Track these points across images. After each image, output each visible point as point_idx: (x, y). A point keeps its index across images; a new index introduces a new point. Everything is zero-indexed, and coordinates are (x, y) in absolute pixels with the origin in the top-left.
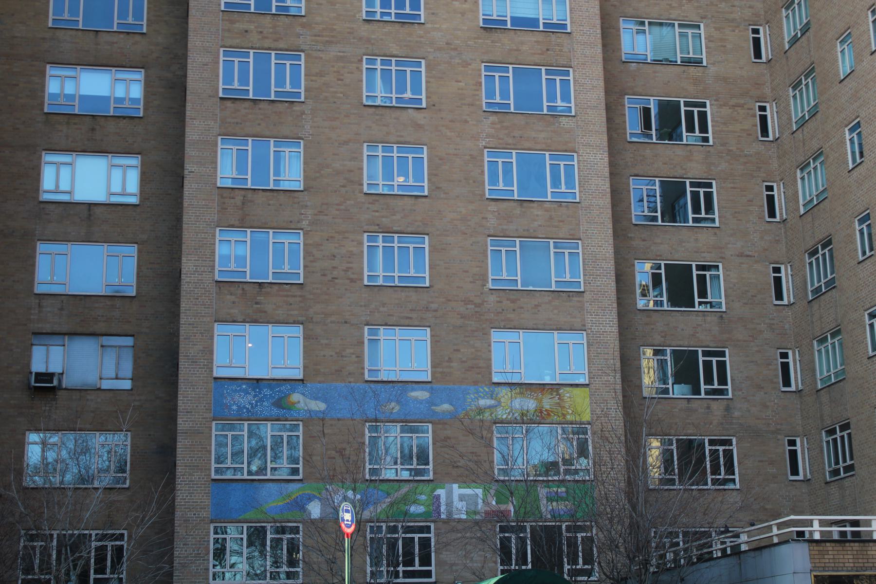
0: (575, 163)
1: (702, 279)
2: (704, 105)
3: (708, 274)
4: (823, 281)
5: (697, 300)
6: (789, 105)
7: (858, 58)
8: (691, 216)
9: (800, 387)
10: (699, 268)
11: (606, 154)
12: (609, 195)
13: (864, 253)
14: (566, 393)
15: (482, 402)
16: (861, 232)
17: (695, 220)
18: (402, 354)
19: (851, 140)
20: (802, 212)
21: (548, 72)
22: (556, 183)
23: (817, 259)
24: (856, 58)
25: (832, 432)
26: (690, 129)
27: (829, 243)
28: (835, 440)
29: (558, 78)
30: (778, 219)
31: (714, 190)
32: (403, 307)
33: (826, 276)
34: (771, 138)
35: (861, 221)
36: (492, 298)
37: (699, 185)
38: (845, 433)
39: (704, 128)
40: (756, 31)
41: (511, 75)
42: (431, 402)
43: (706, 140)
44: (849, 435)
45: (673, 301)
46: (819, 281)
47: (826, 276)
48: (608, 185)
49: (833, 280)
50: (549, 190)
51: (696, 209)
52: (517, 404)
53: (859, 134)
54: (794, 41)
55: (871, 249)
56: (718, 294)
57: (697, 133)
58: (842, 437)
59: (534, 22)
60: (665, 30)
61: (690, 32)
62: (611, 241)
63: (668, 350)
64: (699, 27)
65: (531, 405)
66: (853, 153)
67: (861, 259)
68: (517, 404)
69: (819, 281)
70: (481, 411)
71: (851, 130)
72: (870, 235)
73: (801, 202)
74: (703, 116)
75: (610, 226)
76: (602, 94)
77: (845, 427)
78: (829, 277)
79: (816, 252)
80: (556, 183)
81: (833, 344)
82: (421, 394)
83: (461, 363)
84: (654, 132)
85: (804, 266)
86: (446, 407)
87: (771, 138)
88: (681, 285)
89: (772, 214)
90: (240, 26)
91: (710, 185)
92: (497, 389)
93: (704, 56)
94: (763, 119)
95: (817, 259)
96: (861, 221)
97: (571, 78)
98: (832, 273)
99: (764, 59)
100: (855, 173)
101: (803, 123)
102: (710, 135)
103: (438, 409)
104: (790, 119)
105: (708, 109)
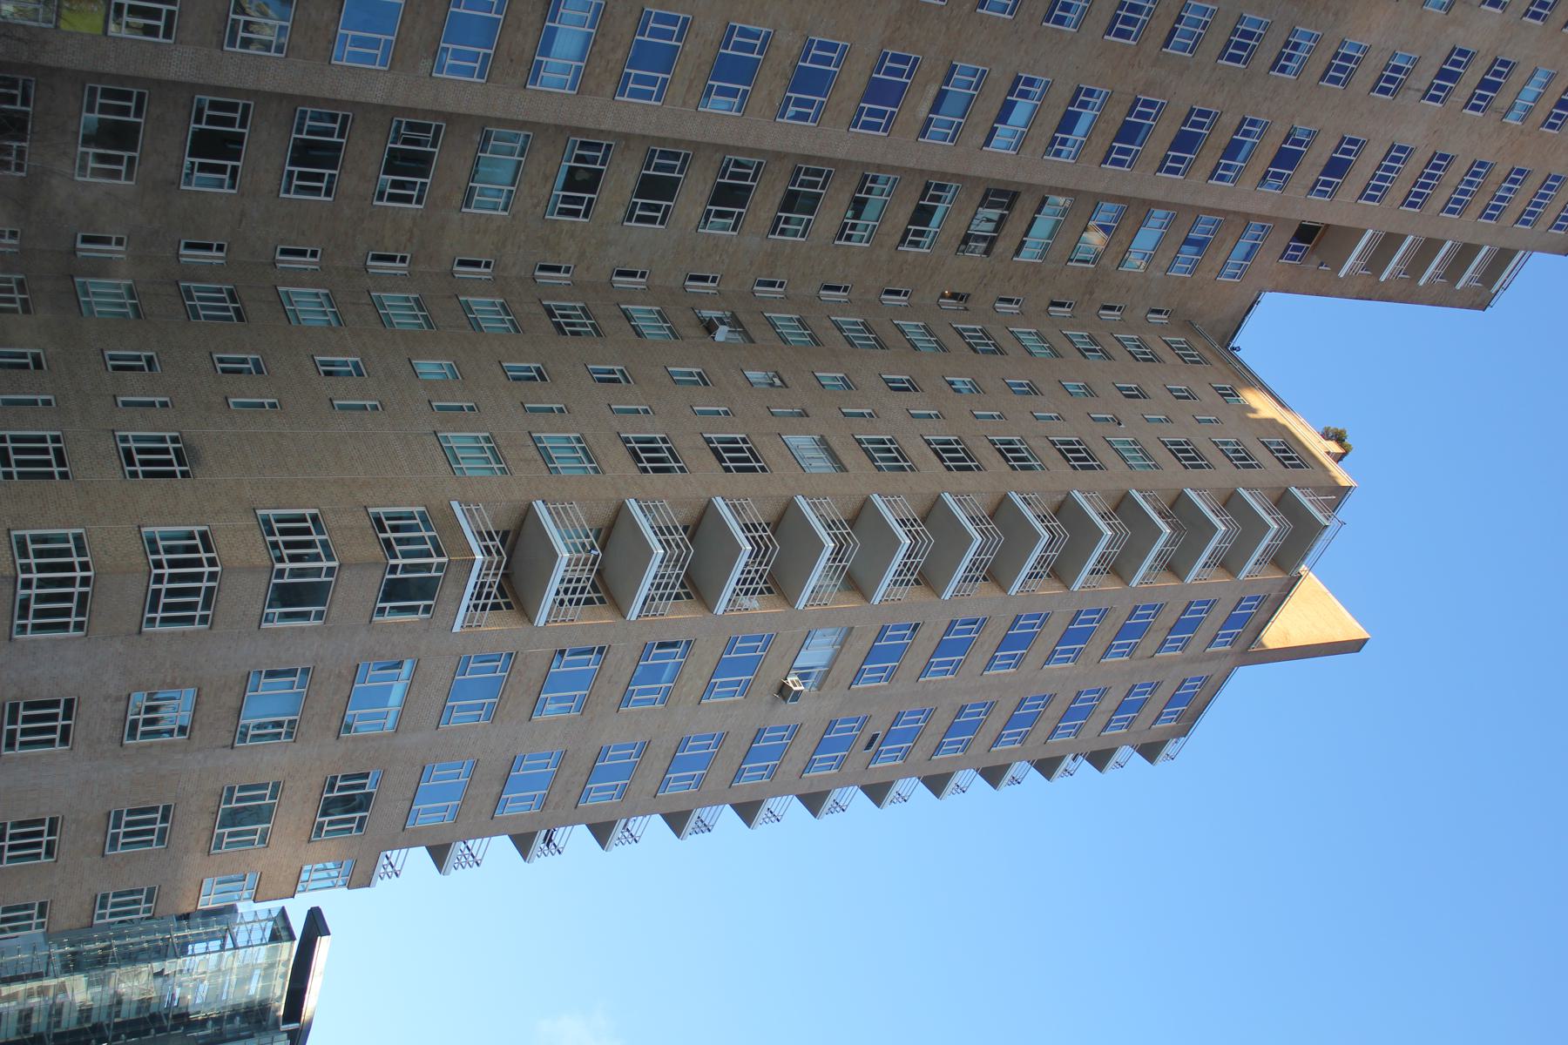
0: (377, 67)
1: (221, 169)
2: (419, 201)
3: (226, 177)
4: (198, 303)
5: (197, 160)
6: (401, 291)
7: (429, 385)
8: (297, 169)
9: (80, 254)
10: (235, 169)
11: (380, 101)
12: (332, 96)
13: (221, 361)
16: (244, 361)
17: (291, 173)
19: (345, 364)
20: (280, 289)
21: (486, 56)
22: (358, 42)
23: (223, 300)
24: (430, 381)
25: (21, 285)
26: (395, 184)
27: (240, 319)
28: (11, 290)
29: (477, 66)
30: (278, 257)
31: (322, 198)
33: (203, 308)
34: (369, 263)
35: (256, 363)
37: (330, 183)
38: (18, 305)
39: (392, 198)
40: (487, 265)
41: (493, 15)
43: (380, 198)
44: (14, 311)
45: (198, 135)
46: (200, 299)
47: (203, 308)
48: (345, 98)
49: (197, 317)
50: (351, 33)
51: (302, 176)
53: (350, 374)
54: (467, 308)
55: (224, 371)
56: (200, 185)
57: (389, 190)
58: (12, 301)
59: (546, 52)
60: (508, 178)
61: (502, 201)
62: (279, 90)
63: (141, 120)
64: (505, 209)
66: (332, 364)
67: (215, 356)
69: (200, 299)
71: (356, 365)
72: (239, 371)
73: (292, 289)
74: (408, 199)
75: (297, 92)
76: (450, 109)
77: (26, 310)
78: (202, 313)
79: (234, 300)
80: (358, 42)
81: (122, 305)
84: (399, 146)
85: (219, 282)
87: (369, 263)
88: (216, 146)
89: (284, 252)
91: (328, 194)
93: (473, 210)
94: (392, 259)
95: (223, 300)
96: (256, 363)
97: (475, 79)
98: (206, 317)
99: (456, 268)
100: (309, 364)
101: (376, 305)
102: (385, 203)
104: (384, 291)
105: (414, 206)
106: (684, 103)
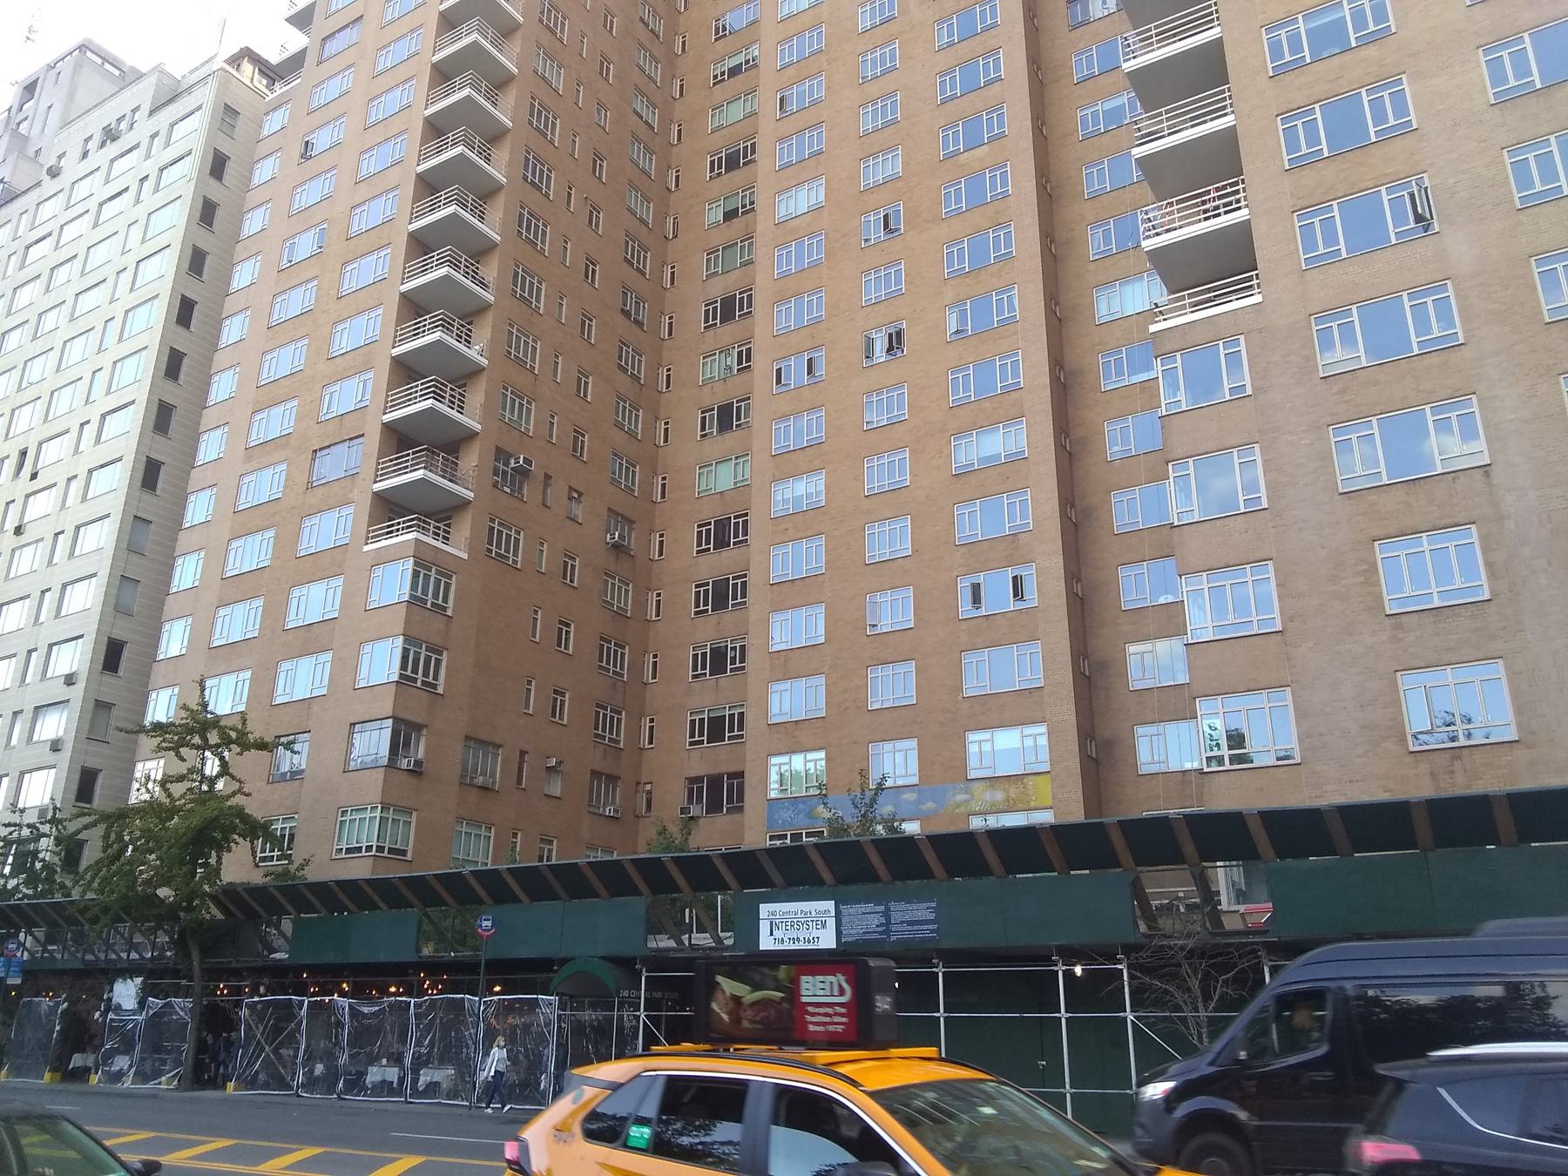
14: (1030, 781)
15: (960, 797)
18: (897, 763)
32: (896, 723)
36: (965, 705)
42: (919, 802)
52: (988, 796)
65: (999, 796)
68: (988, 796)
70: (958, 805)
82: (910, 796)
83: (945, 763)
86: (930, 805)
90: (783, 527)
92: (976, 785)
103: (923, 807)
106: (1016, 333)
